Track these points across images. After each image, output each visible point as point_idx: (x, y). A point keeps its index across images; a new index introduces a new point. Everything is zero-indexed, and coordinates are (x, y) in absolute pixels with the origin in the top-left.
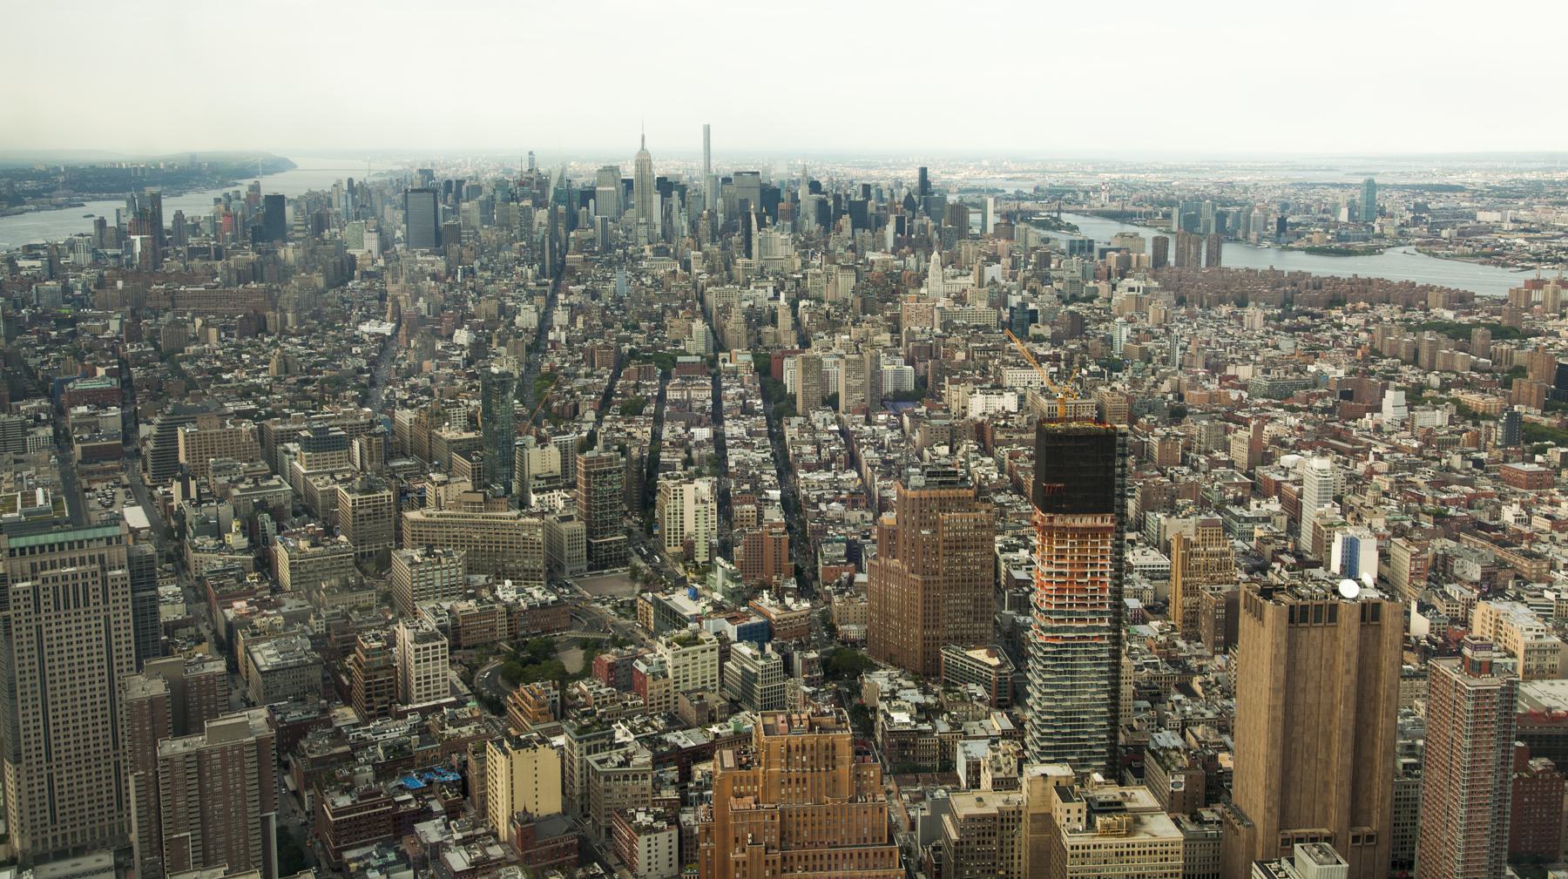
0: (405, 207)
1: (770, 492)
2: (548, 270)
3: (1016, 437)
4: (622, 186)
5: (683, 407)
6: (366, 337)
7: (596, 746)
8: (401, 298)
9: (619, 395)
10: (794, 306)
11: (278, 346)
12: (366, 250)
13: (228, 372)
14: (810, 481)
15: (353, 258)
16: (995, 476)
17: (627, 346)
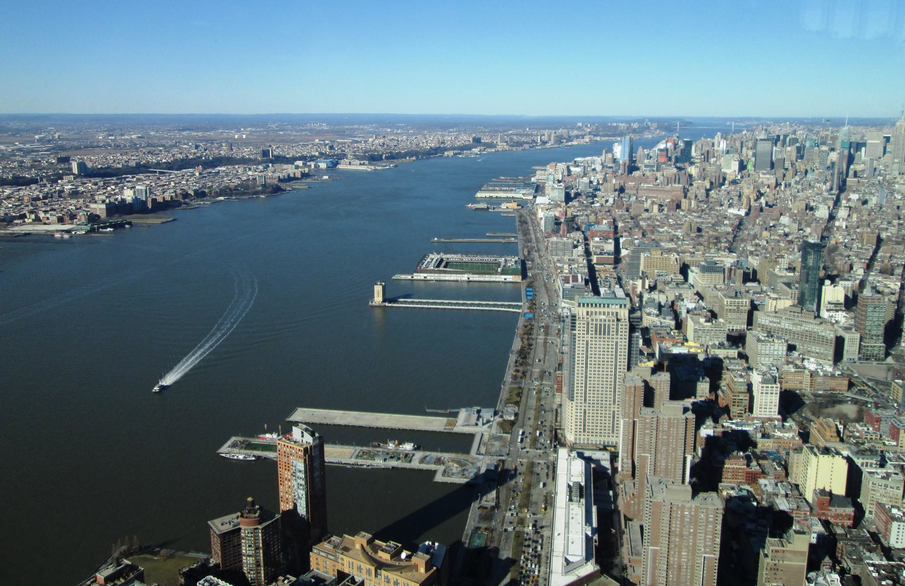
6: (732, 216)
7: (867, 463)
8: (751, 197)
9: (879, 262)
11: (686, 217)
13: (662, 227)
15: (725, 173)
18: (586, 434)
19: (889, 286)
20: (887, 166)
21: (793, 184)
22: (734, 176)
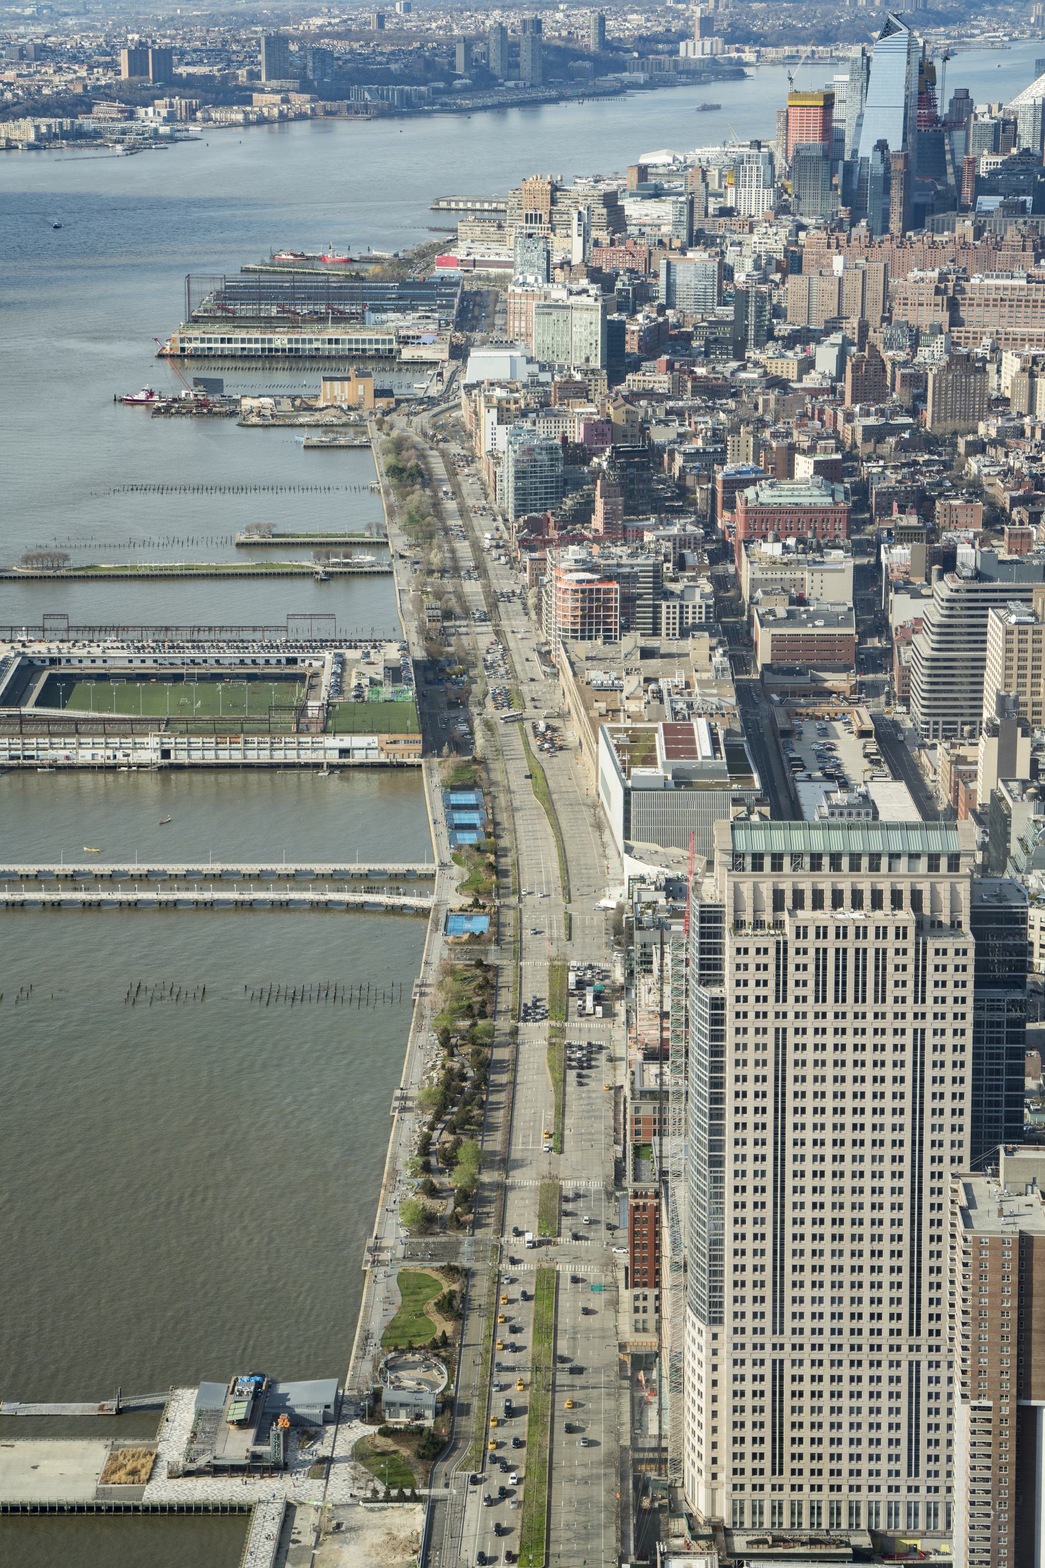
18: (787, 1479)
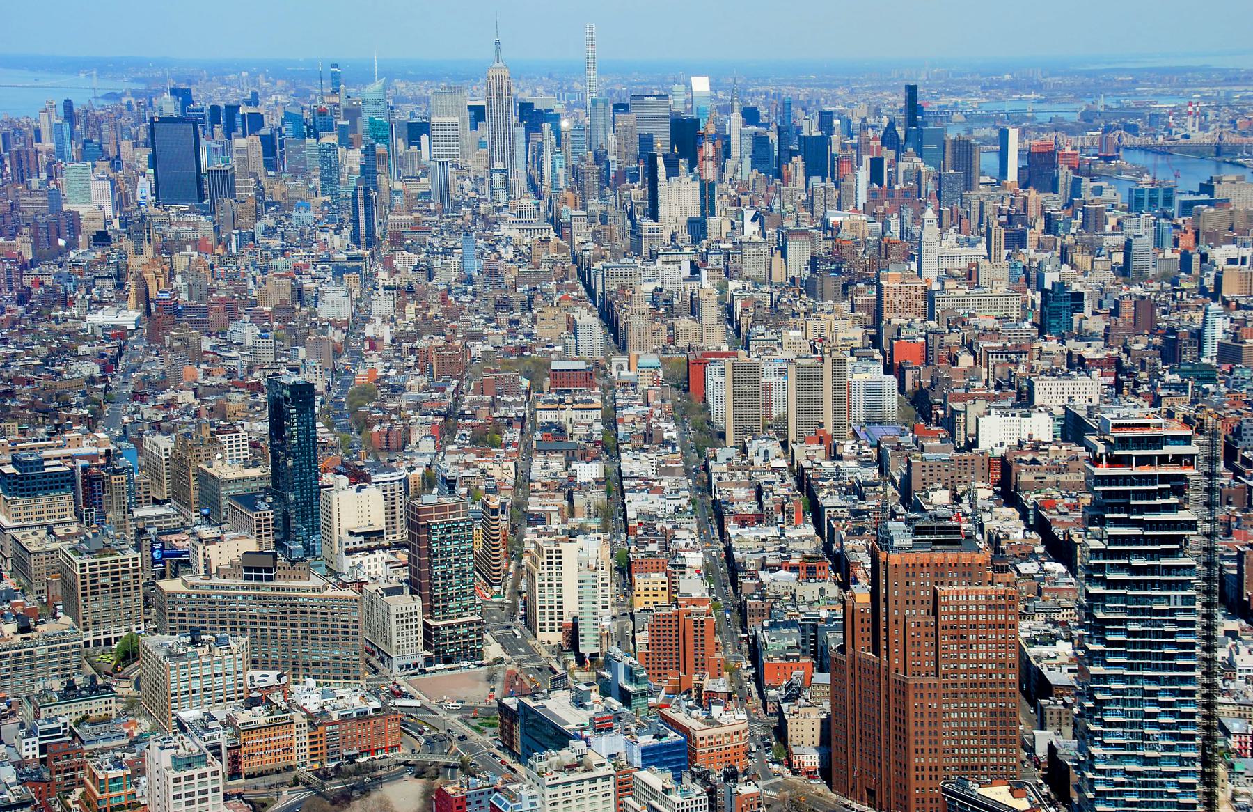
0: (152, 142)
1: (687, 554)
2: (363, 237)
3: (1050, 478)
4: (467, 115)
5: (558, 431)
8: (149, 275)
9: (468, 416)
10: (722, 289)
12: (94, 206)
14: (745, 539)
15: (75, 216)
16: (1020, 535)
17: (479, 345)
19: (490, 473)
20: (482, 179)
21: (258, 236)
22: (101, 223)
